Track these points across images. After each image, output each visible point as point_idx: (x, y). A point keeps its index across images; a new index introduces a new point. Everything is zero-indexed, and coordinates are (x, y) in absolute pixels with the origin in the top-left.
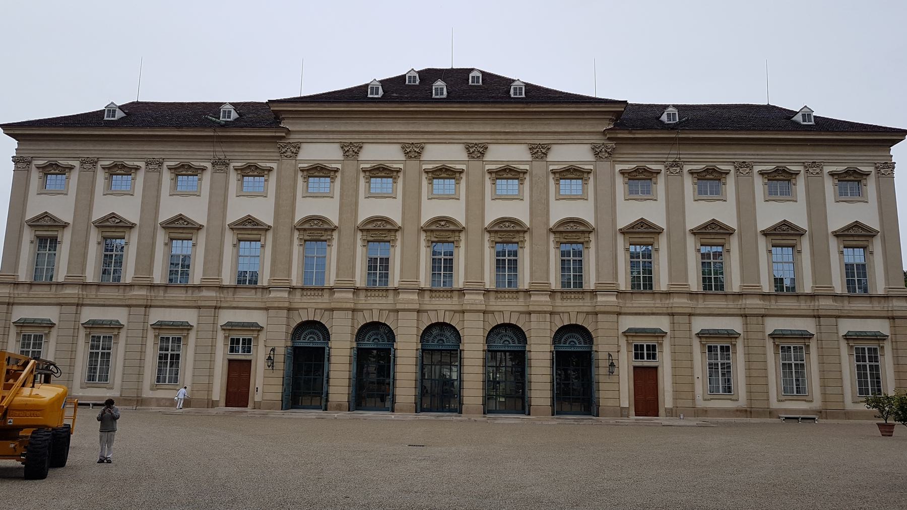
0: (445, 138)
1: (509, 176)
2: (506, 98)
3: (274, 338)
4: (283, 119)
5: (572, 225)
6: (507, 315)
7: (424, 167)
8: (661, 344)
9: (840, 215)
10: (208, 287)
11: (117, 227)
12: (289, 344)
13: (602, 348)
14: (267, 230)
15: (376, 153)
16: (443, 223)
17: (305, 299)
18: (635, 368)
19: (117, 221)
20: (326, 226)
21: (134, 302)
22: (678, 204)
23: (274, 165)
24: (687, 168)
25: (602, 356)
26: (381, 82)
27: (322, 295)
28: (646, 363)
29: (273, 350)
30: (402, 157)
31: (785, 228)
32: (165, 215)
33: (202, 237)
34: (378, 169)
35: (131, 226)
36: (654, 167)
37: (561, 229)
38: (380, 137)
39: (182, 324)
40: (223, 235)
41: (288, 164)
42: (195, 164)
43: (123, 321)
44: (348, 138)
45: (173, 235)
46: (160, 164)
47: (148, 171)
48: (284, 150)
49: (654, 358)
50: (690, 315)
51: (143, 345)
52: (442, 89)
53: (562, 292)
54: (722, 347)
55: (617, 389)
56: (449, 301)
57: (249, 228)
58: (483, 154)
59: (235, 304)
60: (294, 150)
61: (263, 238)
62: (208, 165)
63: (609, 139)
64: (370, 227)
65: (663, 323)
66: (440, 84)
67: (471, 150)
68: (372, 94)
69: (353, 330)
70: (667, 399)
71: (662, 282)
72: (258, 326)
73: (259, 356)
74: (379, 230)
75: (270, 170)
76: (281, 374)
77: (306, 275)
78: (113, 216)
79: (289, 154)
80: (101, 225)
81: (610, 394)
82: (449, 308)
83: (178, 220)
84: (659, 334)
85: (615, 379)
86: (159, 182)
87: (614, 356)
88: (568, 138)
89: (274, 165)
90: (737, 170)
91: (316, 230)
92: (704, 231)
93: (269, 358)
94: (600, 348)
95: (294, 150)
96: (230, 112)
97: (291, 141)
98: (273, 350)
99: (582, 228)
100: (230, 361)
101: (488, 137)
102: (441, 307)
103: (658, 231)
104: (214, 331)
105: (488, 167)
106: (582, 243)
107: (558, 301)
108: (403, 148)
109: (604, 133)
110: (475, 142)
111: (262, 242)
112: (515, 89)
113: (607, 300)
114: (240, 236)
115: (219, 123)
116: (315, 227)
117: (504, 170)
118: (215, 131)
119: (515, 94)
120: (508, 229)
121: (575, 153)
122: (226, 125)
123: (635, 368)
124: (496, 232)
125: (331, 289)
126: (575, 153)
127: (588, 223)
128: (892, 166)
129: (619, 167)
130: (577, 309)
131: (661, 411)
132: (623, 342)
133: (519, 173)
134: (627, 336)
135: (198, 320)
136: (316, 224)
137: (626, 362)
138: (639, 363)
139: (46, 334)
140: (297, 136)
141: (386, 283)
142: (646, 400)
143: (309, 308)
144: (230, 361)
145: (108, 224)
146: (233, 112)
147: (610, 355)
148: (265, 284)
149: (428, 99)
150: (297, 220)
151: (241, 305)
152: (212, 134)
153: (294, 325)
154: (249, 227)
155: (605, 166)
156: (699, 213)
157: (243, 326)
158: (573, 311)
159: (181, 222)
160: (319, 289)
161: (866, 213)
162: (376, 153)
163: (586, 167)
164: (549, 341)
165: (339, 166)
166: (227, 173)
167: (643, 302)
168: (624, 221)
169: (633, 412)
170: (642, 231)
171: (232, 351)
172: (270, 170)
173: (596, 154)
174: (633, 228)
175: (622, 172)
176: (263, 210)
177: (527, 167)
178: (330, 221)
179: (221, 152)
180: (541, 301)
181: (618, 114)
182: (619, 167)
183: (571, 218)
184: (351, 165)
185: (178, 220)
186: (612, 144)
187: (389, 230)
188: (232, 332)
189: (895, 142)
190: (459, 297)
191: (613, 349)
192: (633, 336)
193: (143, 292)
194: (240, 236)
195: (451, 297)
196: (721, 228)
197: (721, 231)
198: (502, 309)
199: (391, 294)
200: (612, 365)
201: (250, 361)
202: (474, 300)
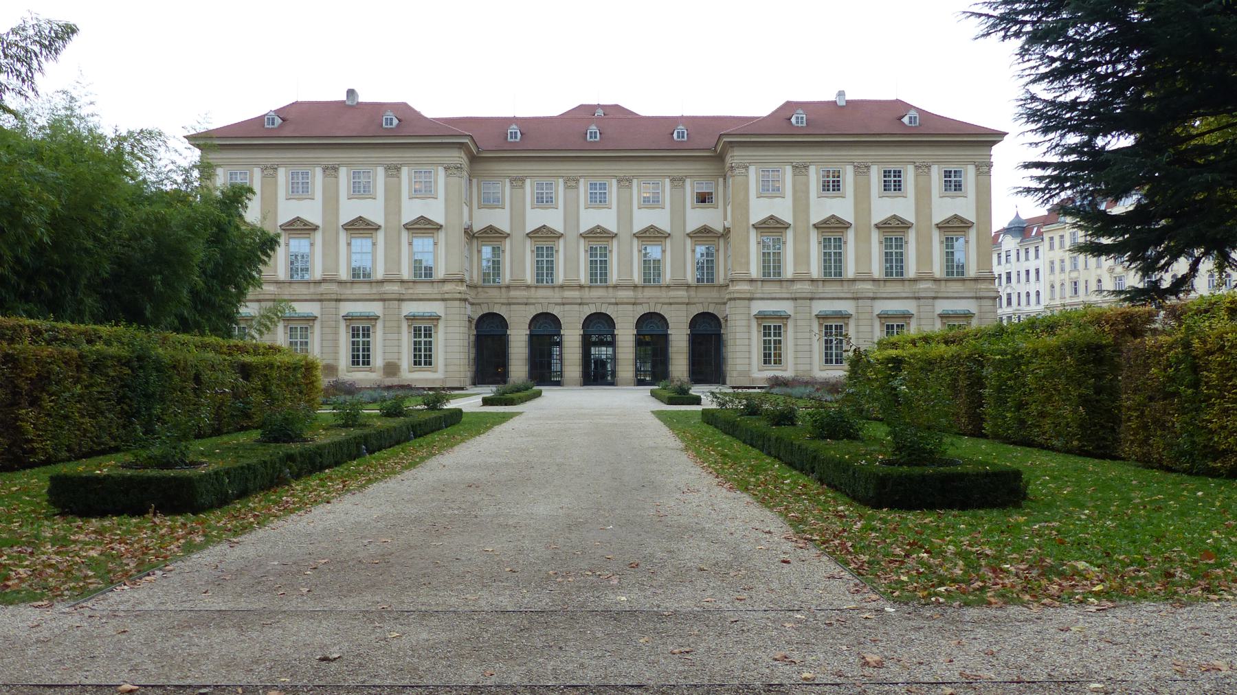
9: (944, 208)
32: (345, 218)
33: (380, 236)
35: (316, 228)
51: (336, 333)
57: (360, 227)
103: (786, 227)
104: (399, 321)
128: (990, 165)
161: (964, 207)
176: (373, 210)
189: (995, 143)
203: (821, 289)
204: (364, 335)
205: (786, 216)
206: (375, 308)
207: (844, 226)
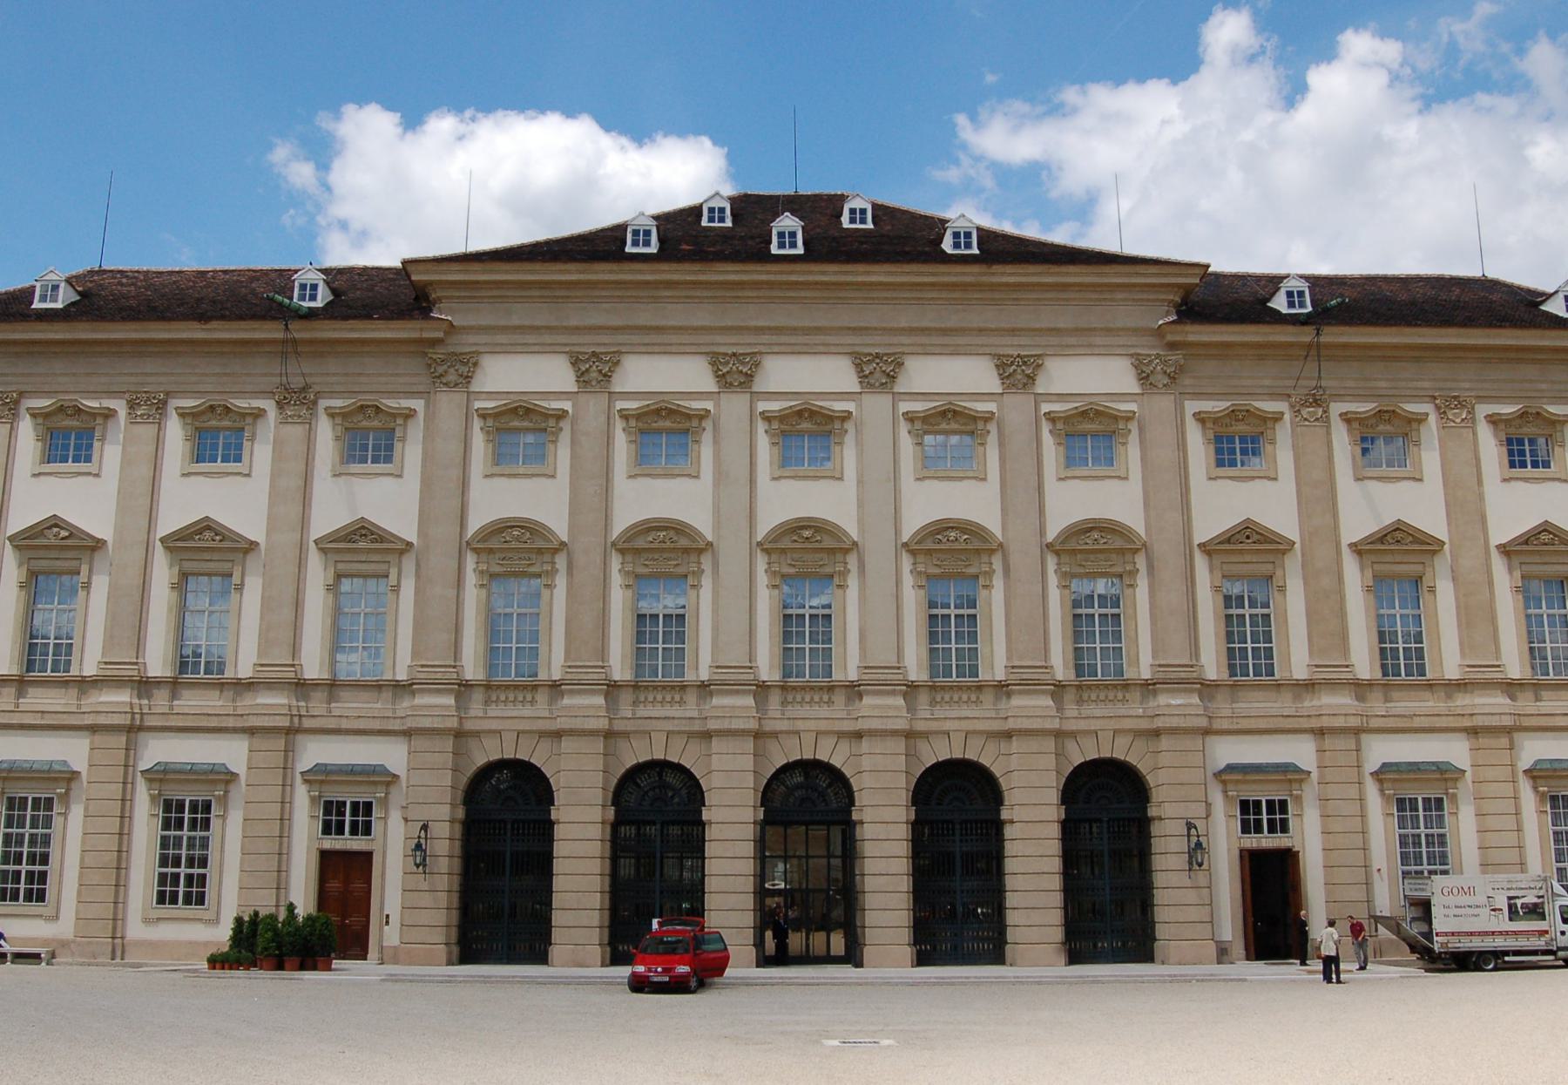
0: (805, 341)
1: (954, 426)
2: (935, 255)
4: (439, 300)
7: (762, 406)
8: (1298, 799)
10: (271, 685)
11: (63, 548)
13: (1168, 812)
14: (402, 552)
15: (650, 375)
16: (807, 533)
17: (494, 711)
19: (64, 533)
20: (540, 544)
21: (102, 720)
22: (1320, 490)
23: (418, 404)
24: (1336, 408)
26: (656, 218)
27: (533, 702)
28: (1266, 841)
29: (425, 827)
30: (710, 385)
31: (1545, 537)
32: (172, 520)
34: (657, 412)
36: (1269, 406)
37: (1072, 545)
38: (659, 340)
41: (449, 404)
42: (242, 403)
43: (79, 763)
44: (587, 343)
45: (188, 566)
46: (161, 406)
47: (133, 420)
48: (441, 370)
49: (1285, 829)
50: (1357, 732)
52: (793, 235)
54: (1426, 801)
56: (824, 711)
58: (892, 378)
59: (331, 724)
61: (393, 572)
62: (269, 405)
63: (1172, 346)
64: (641, 543)
65: (1301, 752)
66: (788, 222)
68: (635, 243)
69: (606, 780)
71: (1297, 659)
73: (391, 843)
74: (664, 551)
75: (410, 414)
76: (443, 882)
77: (492, 654)
78: (55, 523)
79: (452, 377)
80: (28, 542)
82: (823, 726)
85: (1201, 878)
86: (159, 441)
87: (1200, 824)
88: (1083, 340)
90: (1442, 414)
91: (516, 551)
93: (418, 846)
94: (1168, 810)
96: (314, 287)
97: (459, 349)
98: (425, 827)
99: (1118, 543)
100: (325, 855)
101: (905, 340)
102: (812, 725)
104: (286, 785)
105: (904, 407)
106: (1121, 576)
107: (1071, 710)
108: (713, 364)
109: (1159, 332)
110: (874, 351)
111: (393, 579)
113: (1177, 705)
114: (341, 566)
115: (288, 307)
116: (514, 545)
117: (943, 414)
120: (956, 546)
121: (1096, 376)
122: (312, 314)
124: (929, 552)
125: (555, 687)
126: (1096, 376)
127: (1130, 530)
133: (975, 419)
136: (518, 539)
137: (1226, 841)
139: (60, 796)
140: (472, 339)
141: (680, 670)
143: (505, 732)
144: (325, 855)
145: (43, 541)
147: (1190, 826)
149: (761, 255)
150: (470, 533)
151: (345, 724)
153: (470, 771)
154: (362, 545)
155: (1163, 403)
156: (1366, 507)
157: (347, 773)
158: (1104, 732)
159: (208, 534)
160: (525, 687)
162: (650, 375)
163: (1124, 407)
164: (1054, 796)
165: (567, 405)
166: (310, 423)
167: (1257, 705)
170: (1248, 545)
171: (327, 830)
172: (410, 414)
173: (1144, 378)
174: (1228, 541)
177: (991, 407)
178: (550, 530)
179: (300, 371)
180: (1032, 708)
181: (1188, 290)
182: (1191, 407)
184: (594, 406)
186: (1176, 357)
187: (686, 551)
188: (325, 788)
190: (849, 700)
191: (1196, 811)
193: (123, 697)
194: (341, 566)
195: (830, 702)
196: (1416, 541)
197: (1416, 547)
199: (691, 697)
200: (1199, 845)
201: (367, 856)
202: (882, 709)
203: (1376, 705)
204: (193, 827)
206: (232, 753)
207: (1427, 546)
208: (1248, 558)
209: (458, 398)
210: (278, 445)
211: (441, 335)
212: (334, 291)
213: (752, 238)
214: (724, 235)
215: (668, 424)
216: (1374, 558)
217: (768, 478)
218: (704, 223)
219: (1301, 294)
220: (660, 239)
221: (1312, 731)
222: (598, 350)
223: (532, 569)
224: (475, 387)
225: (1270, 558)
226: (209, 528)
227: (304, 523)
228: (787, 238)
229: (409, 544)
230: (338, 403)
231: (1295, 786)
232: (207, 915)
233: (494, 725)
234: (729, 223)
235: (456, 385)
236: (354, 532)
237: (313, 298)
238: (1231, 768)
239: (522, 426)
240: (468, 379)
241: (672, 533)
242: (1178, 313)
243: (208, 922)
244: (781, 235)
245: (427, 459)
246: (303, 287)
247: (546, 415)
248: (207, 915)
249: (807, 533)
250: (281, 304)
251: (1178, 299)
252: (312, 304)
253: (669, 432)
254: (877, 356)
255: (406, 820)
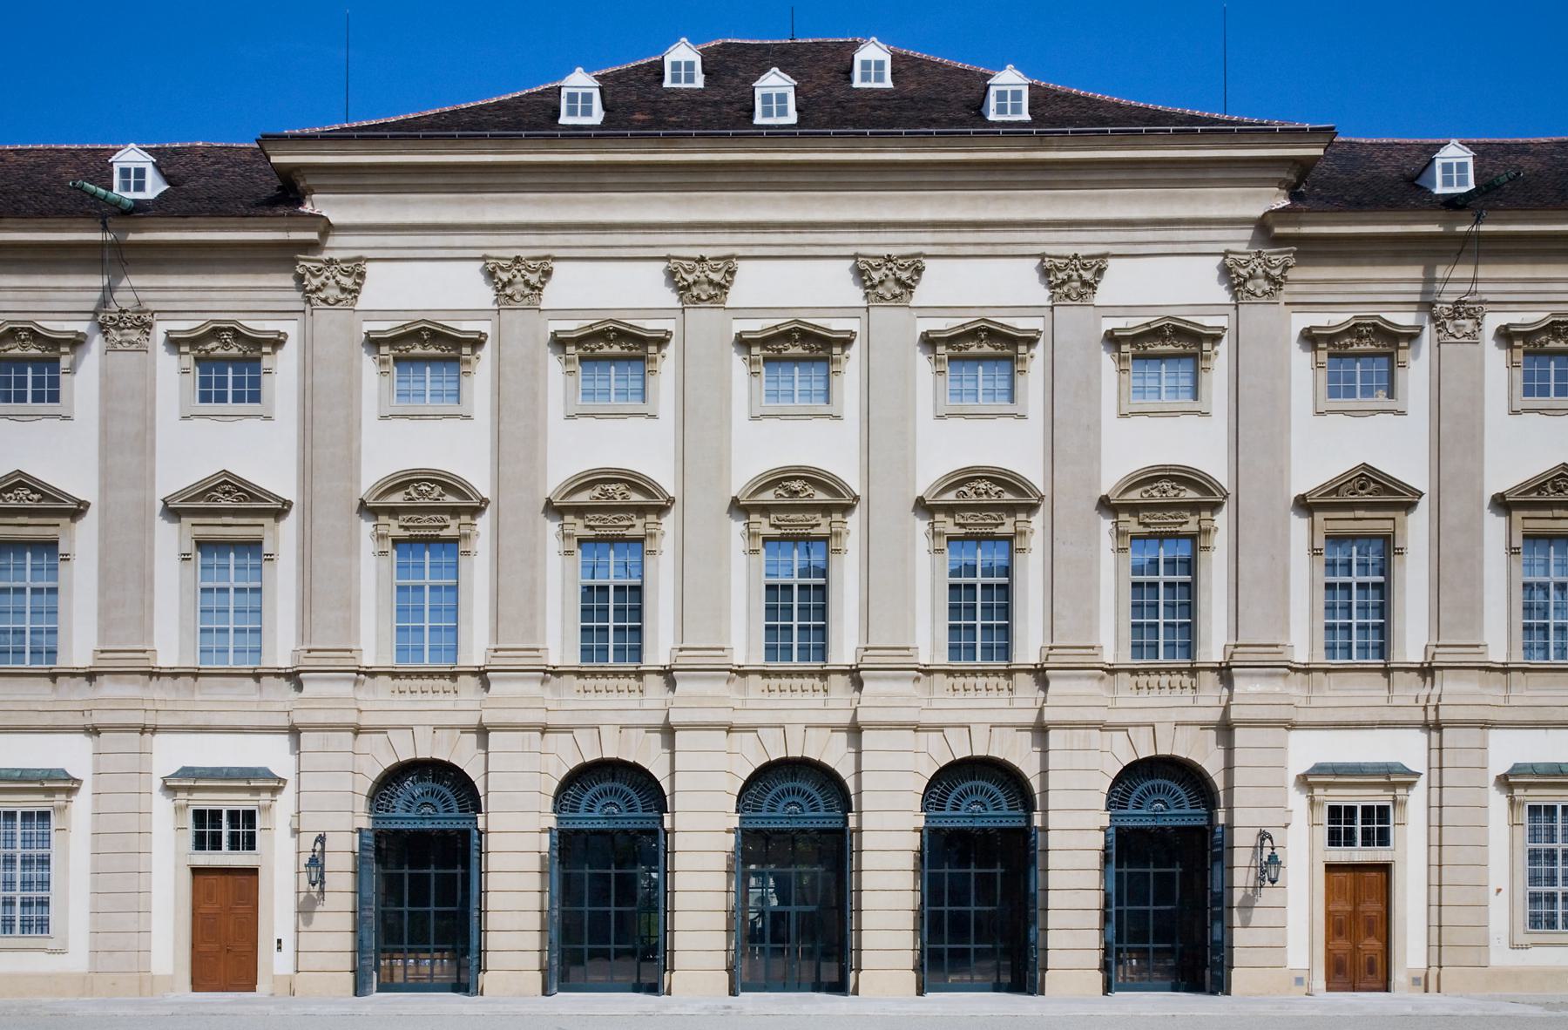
3: (317, 815)
4: (311, 190)
5: (1165, 485)
6: (980, 734)
12: (365, 823)
13: (1245, 820)
16: (796, 485)
18: (1330, 868)
23: (290, 327)
24: (1493, 321)
25: (1243, 838)
28: (1359, 854)
39: (51, 775)
40: (147, 529)
52: (782, 98)
53: (1134, 672)
55: (1281, 926)
59: (199, 720)
60: (347, 282)
66: (775, 82)
67: (876, 276)
68: (572, 112)
70: (1411, 948)
72: (274, 777)
73: (277, 860)
81: (1261, 937)
83: (10, 489)
84: (1394, 777)
89: (290, 327)
92: (1534, 496)
95: (347, 282)
96: (140, 173)
97: (337, 255)
110: (884, 251)
112: (1001, 95)
118: (105, 229)
119: (1001, 110)
120: (984, 499)
122: (140, 208)
123: (1330, 868)
129: (1302, 321)
130: (1176, 716)
131: (1399, 977)
132: (1298, 801)
134: (1311, 787)
135: (96, 764)
137: (1304, 851)
138: (1342, 855)
142: (1359, 945)
146: (150, 173)
148: (284, 662)
151: (217, 720)
152: (97, 236)
154: (226, 503)
168: (1312, 472)
169: (1319, 981)
172: (277, 342)
175: (1311, 338)
183: (1164, 468)
185: (10, 489)
192: (1327, 785)
198: (965, 718)
205: (1407, 464)
208: (1359, 514)
209: (339, 316)
210: (106, 378)
211: (314, 236)
212: (168, 178)
213: (730, 103)
214: (692, 99)
215: (616, 349)
216: (1526, 513)
217: (745, 415)
218: (667, 84)
219: (1462, 167)
220: (605, 107)
221: (1426, 726)
222: (523, 254)
223: (445, 533)
224: (364, 302)
225: (1391, 514)
226: (20, 484)
227: (146, 478)
228: (775, 102)
229: (289, 504)
230: (182, 326)
231: (1400, 791)
232: (51, 944)
233: (405, 719)
234: (699, 82)
235: (339, 301)
236: (214, 489)
237: (140, 187)
238: (1319, 769)
239: (427, 349)
240: (354, 292)
241: (622, 487)
242: (1294, 195)
243: (53, 952)
244: (767, 98)
245: (307, 395)
246: (125, 172)
247: (457, 342)
248: (51, 944)
249: (796, 485)
250: (93, 195)
251: (1292, 178)
252: (139, 196)
253: (613, 359)
254: (889, 258)
255: (296, 832)
